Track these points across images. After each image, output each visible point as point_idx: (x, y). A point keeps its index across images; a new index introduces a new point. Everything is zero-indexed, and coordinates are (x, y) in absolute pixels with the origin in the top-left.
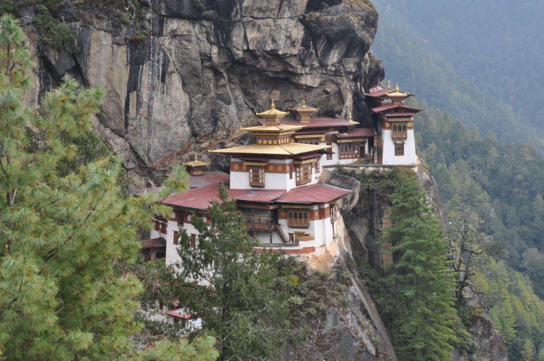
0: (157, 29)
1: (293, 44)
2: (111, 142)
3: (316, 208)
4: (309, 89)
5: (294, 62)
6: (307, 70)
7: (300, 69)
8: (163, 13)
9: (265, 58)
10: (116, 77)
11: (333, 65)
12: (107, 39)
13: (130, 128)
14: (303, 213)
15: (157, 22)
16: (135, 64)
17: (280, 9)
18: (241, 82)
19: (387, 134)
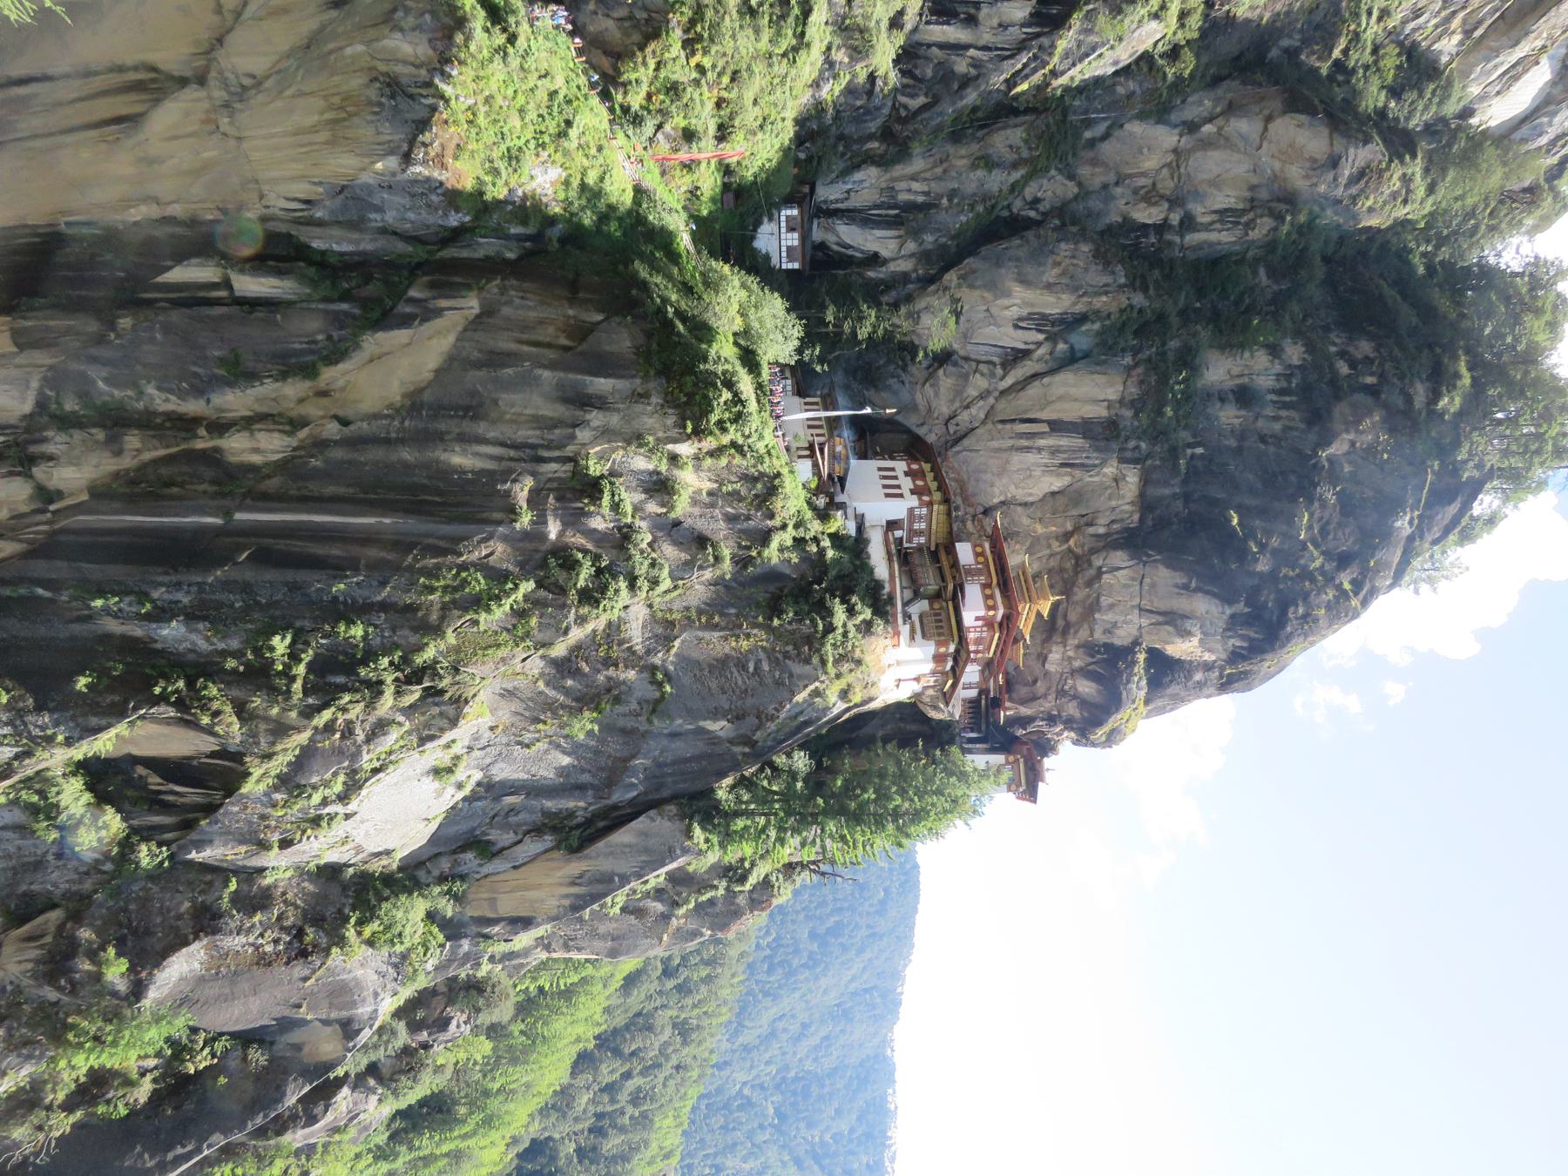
0: (1128, 455)
1: (1108, 631)
2: (981, 403)
3: (952, 648)
4: (1043, 659)
5: (1083, 634)
6: (1071, 653)
7: (1073, 642)
8: (1149, 462)
9: (1089, 596)
10: (1066, 406)
11: (1074, 687)
12: (1113, 393)
13: (1000, 426)
14: (945, 630)
15: (1136, 455)
16: (1085, 428)
17: (1151, 612)
18: (1050, 572)
19: (998, 759)
